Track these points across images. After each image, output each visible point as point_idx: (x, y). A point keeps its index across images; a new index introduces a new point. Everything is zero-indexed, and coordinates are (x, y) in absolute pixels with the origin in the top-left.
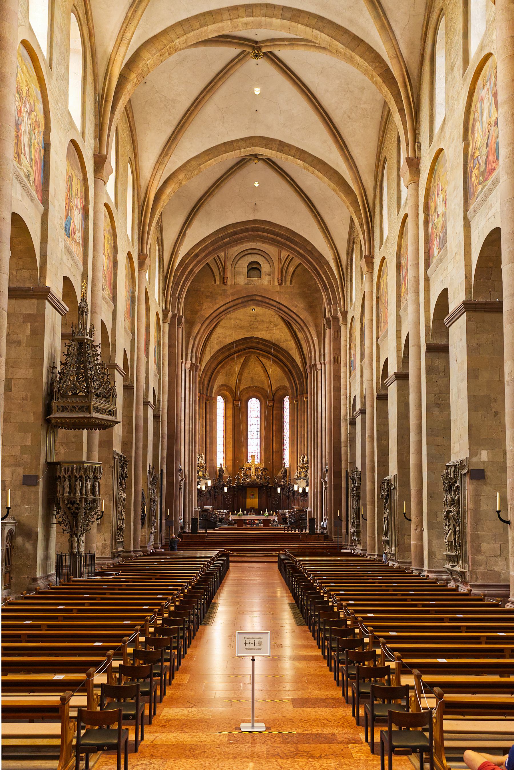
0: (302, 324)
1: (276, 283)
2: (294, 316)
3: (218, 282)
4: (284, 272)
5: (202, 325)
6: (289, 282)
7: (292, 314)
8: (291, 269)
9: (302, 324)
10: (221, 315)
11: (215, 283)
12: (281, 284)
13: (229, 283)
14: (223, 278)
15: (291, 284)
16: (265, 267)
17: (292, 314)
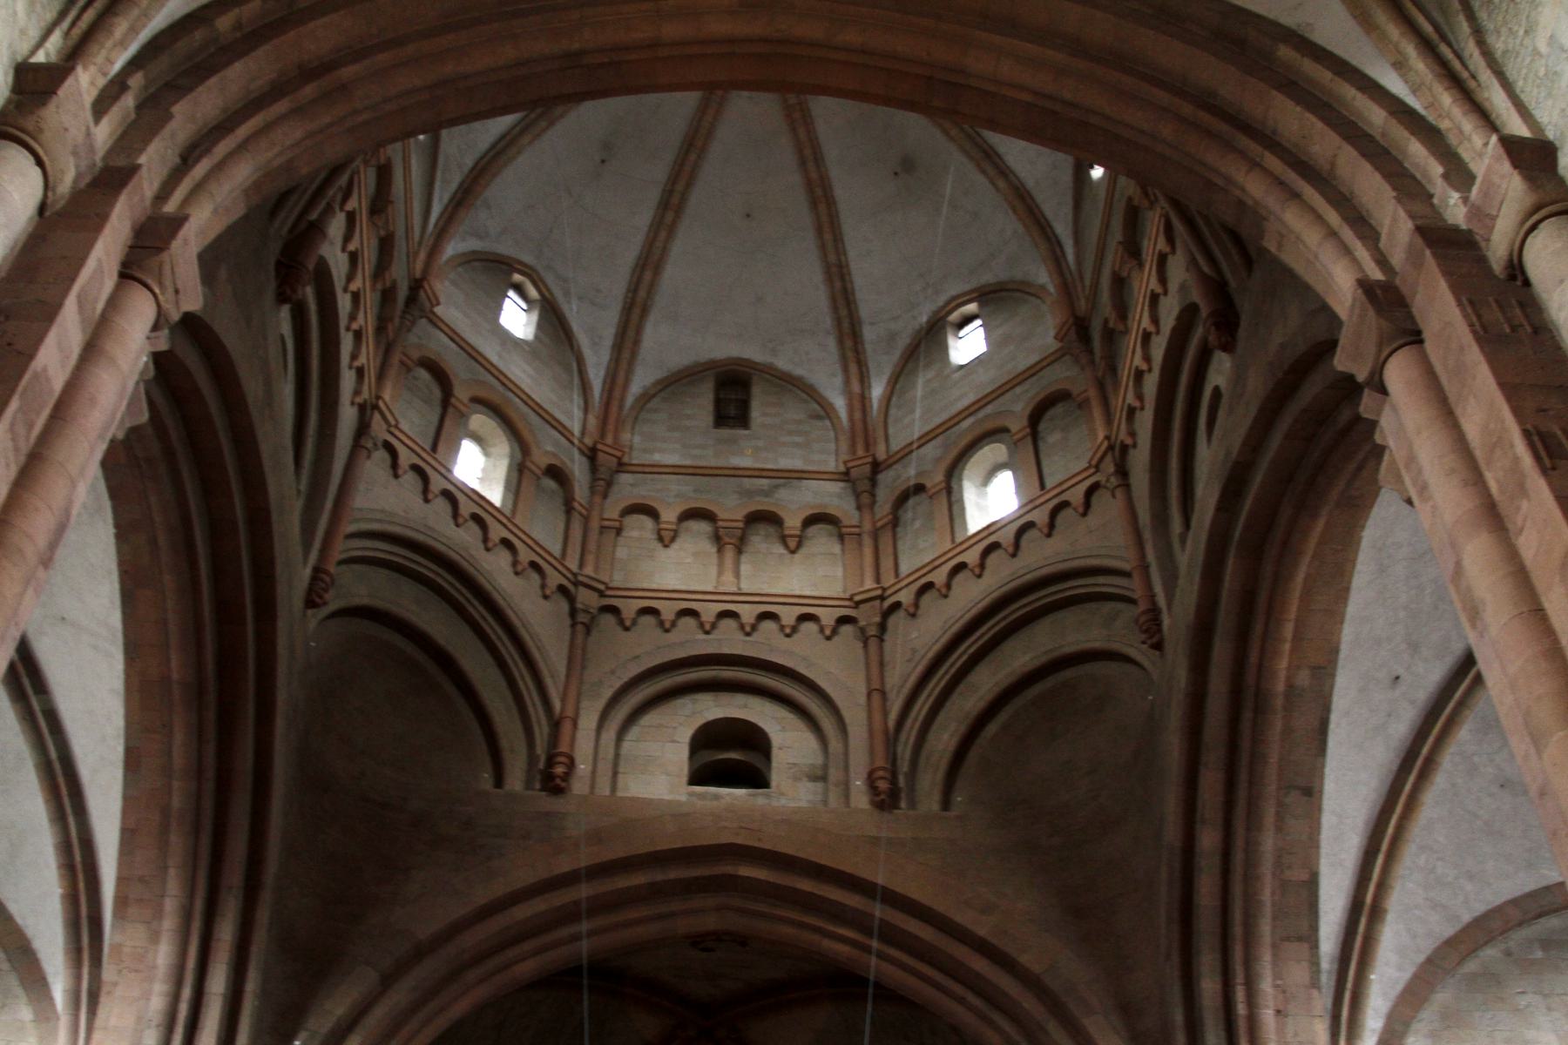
0: (1029, 1003)
1: (861, 799)
2: (980, 965)
3: (515, 780)
4: (905, 751)
5: (388, 981)
6: (936, 797)
7: (961, 952)
8: (944, 739)
9: (1029, 1003)
10: (511, 953)
11: (499, 781)
12: (887, 798)
13: (579, 786)
14: (551, 761)
15: (946, 804)
16: (791, 744)
17: (961, 952)
